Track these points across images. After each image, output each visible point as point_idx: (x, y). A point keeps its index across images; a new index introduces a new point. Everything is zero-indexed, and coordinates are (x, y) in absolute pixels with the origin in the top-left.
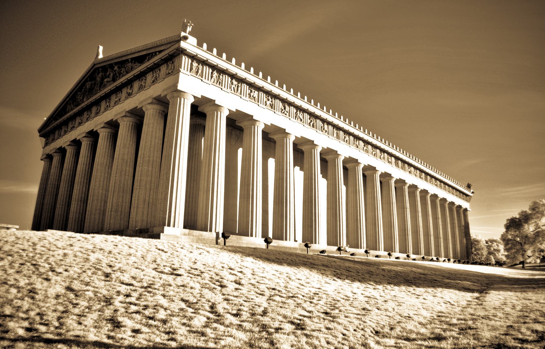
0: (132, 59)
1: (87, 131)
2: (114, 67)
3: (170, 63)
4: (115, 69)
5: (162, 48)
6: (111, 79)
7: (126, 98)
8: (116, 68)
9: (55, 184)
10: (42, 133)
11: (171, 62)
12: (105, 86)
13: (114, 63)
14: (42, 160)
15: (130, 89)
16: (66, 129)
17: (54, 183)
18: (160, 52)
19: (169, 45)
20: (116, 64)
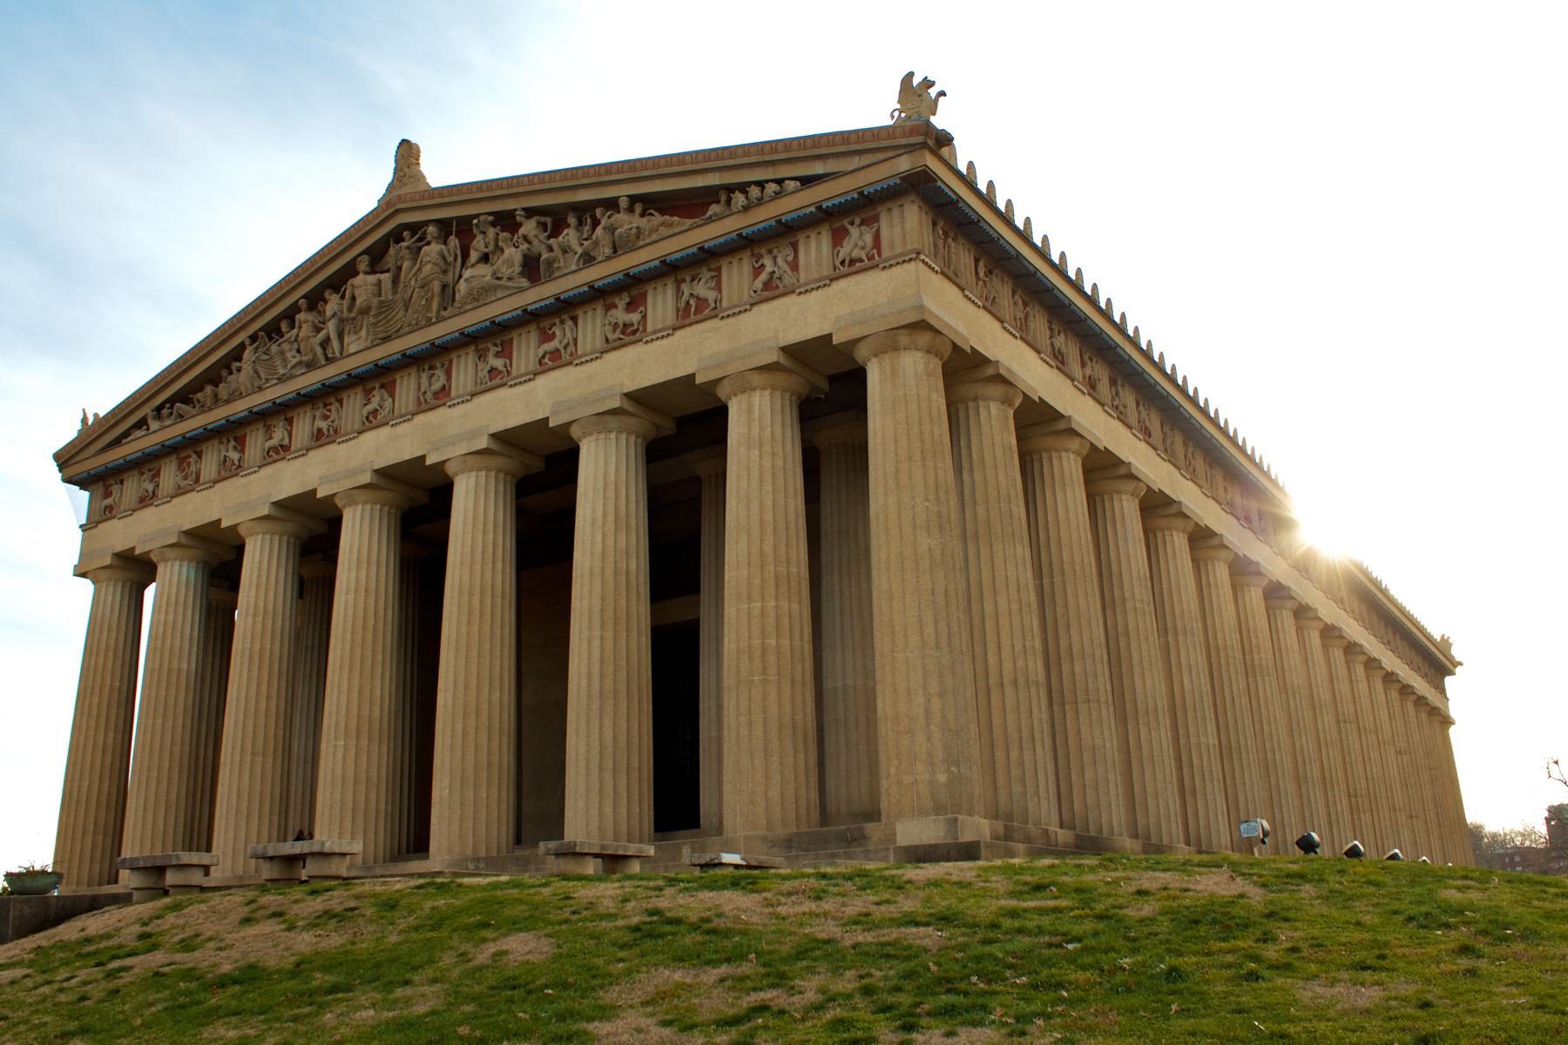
0: (634, 199)
1: (381, 463)
2: (520, 225)
3: (852, 223)
4: (522, 231)
5: (818, 168)
6: (518, 269)
7: (611, 346)
8: (529, 227)
9: (179, 671)
10: (77, 470)
11: (857, 221)
12: (480, 296)
13: (524, 209)
14: (84, 575)
15: (630, 307)
16: (234, 456)
17: (175, 665)
18: (807, 181)
19: (855, 162)
20: (530, 212)
